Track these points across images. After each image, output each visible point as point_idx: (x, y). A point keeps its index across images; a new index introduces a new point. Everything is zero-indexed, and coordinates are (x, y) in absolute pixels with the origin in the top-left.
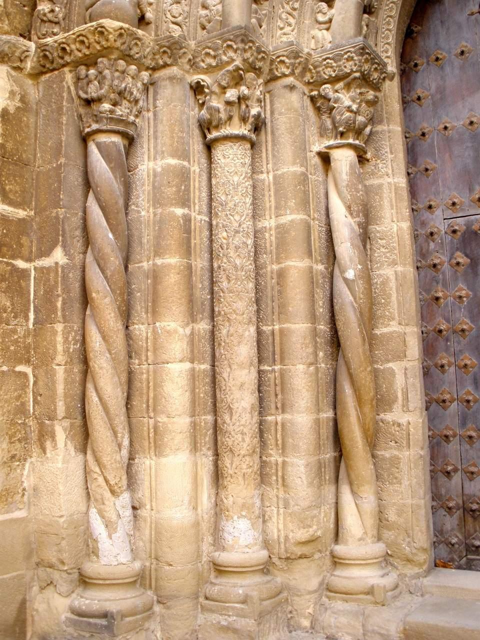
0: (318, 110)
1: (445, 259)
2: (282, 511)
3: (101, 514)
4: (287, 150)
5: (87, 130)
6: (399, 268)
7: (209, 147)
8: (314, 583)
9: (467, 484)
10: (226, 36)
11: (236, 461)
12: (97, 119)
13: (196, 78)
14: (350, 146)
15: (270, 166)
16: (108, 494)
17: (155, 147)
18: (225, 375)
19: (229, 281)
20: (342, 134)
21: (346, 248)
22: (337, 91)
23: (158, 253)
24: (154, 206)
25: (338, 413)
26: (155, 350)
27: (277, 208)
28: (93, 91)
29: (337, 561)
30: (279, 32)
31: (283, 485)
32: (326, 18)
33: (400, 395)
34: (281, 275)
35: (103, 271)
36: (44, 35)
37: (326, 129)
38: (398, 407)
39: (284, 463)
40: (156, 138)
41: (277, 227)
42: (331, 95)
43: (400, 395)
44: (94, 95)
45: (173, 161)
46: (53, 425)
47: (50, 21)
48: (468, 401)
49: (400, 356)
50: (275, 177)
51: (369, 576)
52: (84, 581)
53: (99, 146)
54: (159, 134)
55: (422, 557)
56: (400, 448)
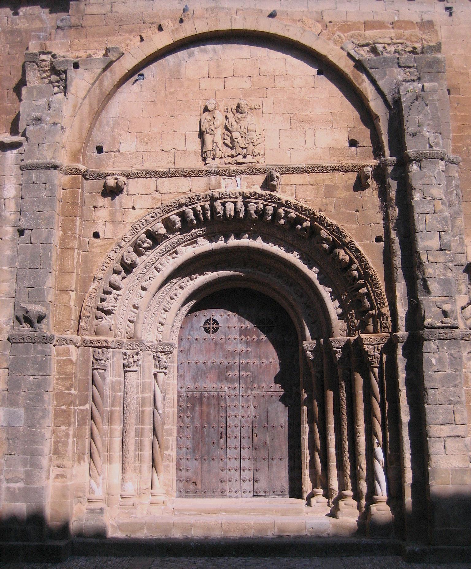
0: (155, 359)
1: (185, 404)
2: (139, 480)
3: (95, 481)
4: (147, 375)
5: (95, 367)
6: (173, 409)
7: (125, 372)
8: (148, 502)
9: (186, 473)
10: (137, 342)
11: (129, 466)
12: (99, 365)
13: (125, 351)
14: (163, 372)
15: (141, 378)
16: (98, 476)
17: (113, 373)
18: (127, 441)
19: (130, 413)
20: (162, 369)
21: (159, 404)
22: (161, 355)
23: (113, 405)
24: (112, 391)
25: (154, 452)
26: (111, 434)
27: (143, 391)
28: (100, 357)
29: (153, 495)
30: (147, 334)
31: (140, 472)
32: (161, 331)
33: (171, 446)
34: (143, 412)
35: (99, 411)
37: (157, 366)
38: (170, 450)
39: (140, 466)
40: (113, 370)
41: (142, 397)
42: (160, 356)
43: (171, 446)
44: (101, 359)
45: (118, 379)
46: (84, 456)
48: (188, 448)
49: (171, 435)
50: (142, 382)
51: (161, 498)
52: (89, 501)
53: (98, 372)
54: (114, 369)
55: (175, 494)
56: (170, 462)
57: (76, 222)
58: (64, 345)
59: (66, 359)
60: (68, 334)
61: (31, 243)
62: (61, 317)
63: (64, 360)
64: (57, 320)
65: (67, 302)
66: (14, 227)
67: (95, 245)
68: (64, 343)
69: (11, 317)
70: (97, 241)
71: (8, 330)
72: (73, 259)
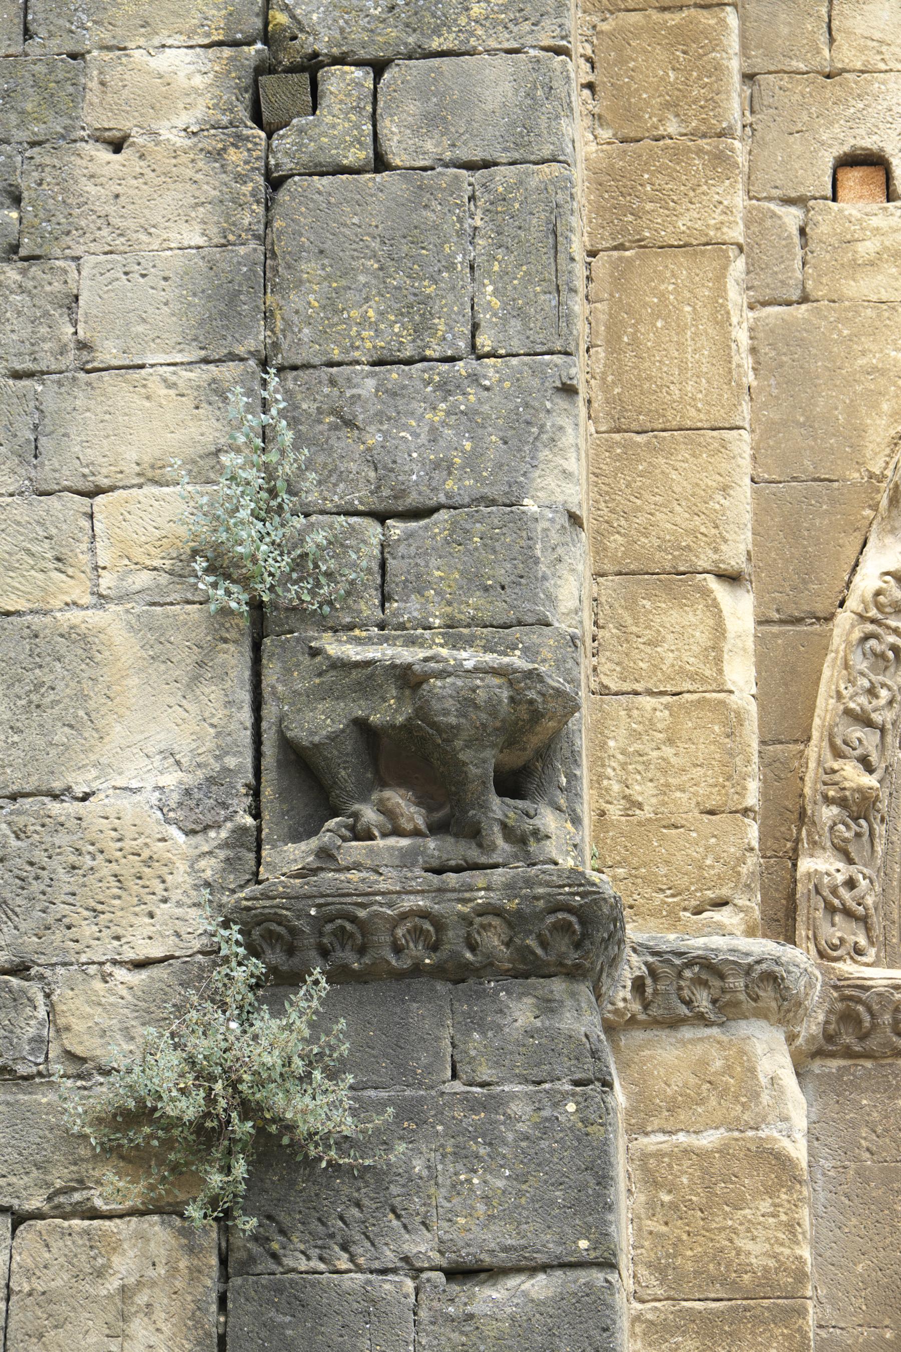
36: (835, 948)
47: (848, 913)
57: (716, 45)
58: (702, 1020)
59: (723, 1150)
60: (721, 930)
61: (380, 163)
62: (642, 791)
63: (702, 1155)
64: (614, 811)
65: (693, 663)
66: (227, 52)
67: (867, 248)
68: (702, 999)
69: (231, 762)
70: (875, 222)
71: (209, 868)
72: (723, 322)
